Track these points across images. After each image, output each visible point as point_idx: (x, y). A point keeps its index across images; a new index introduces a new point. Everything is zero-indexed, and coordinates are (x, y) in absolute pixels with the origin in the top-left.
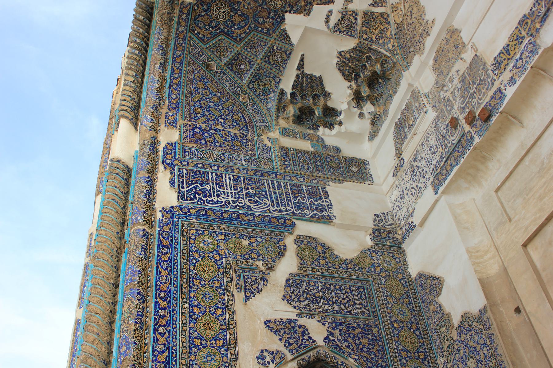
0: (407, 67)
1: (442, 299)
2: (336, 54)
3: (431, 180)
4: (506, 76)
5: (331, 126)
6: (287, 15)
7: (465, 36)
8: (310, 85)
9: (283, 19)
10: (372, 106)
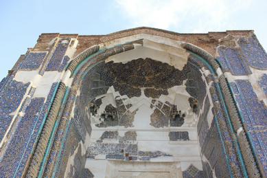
0: (120, 125)
4: (140, 157)
5: (93, 114)
7: (137, 138)
8: (99, 102)
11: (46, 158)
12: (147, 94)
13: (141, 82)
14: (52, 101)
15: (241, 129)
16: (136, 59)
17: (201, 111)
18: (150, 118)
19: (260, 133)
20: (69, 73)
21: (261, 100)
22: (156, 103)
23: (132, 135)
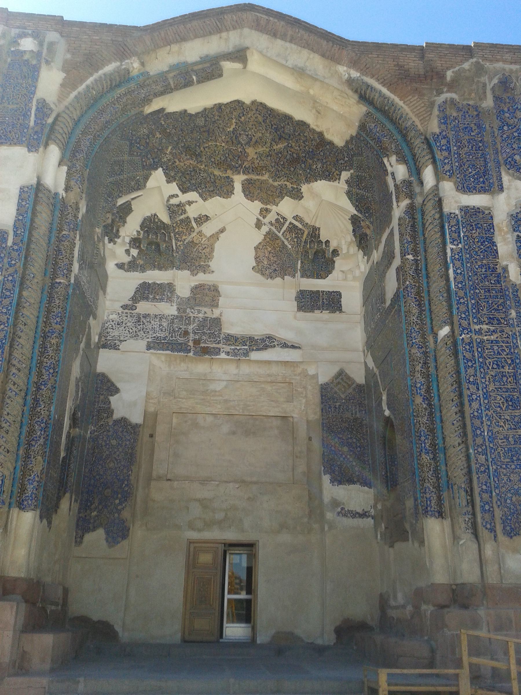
0: (178, 268)
1: (114, 400)
2: (153, 213)
3: (150, 340)
6: (160, 169)
9: (156, 169)
10: (137, 254)
11: (34, 378)
12: (249, 191)
13: (234, 162)
14: (26, 239)
15: (445, 331)
16: (225, 99)
17: (376, 255)
18: (253, 253)
19: (482, 341)
20: (54, 152)
21: (505, 263)
22: (271, 217)
23: (206, 295)
